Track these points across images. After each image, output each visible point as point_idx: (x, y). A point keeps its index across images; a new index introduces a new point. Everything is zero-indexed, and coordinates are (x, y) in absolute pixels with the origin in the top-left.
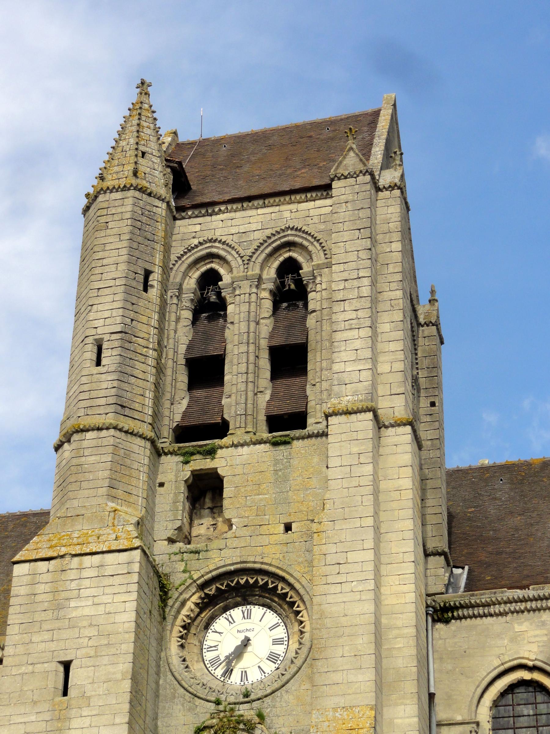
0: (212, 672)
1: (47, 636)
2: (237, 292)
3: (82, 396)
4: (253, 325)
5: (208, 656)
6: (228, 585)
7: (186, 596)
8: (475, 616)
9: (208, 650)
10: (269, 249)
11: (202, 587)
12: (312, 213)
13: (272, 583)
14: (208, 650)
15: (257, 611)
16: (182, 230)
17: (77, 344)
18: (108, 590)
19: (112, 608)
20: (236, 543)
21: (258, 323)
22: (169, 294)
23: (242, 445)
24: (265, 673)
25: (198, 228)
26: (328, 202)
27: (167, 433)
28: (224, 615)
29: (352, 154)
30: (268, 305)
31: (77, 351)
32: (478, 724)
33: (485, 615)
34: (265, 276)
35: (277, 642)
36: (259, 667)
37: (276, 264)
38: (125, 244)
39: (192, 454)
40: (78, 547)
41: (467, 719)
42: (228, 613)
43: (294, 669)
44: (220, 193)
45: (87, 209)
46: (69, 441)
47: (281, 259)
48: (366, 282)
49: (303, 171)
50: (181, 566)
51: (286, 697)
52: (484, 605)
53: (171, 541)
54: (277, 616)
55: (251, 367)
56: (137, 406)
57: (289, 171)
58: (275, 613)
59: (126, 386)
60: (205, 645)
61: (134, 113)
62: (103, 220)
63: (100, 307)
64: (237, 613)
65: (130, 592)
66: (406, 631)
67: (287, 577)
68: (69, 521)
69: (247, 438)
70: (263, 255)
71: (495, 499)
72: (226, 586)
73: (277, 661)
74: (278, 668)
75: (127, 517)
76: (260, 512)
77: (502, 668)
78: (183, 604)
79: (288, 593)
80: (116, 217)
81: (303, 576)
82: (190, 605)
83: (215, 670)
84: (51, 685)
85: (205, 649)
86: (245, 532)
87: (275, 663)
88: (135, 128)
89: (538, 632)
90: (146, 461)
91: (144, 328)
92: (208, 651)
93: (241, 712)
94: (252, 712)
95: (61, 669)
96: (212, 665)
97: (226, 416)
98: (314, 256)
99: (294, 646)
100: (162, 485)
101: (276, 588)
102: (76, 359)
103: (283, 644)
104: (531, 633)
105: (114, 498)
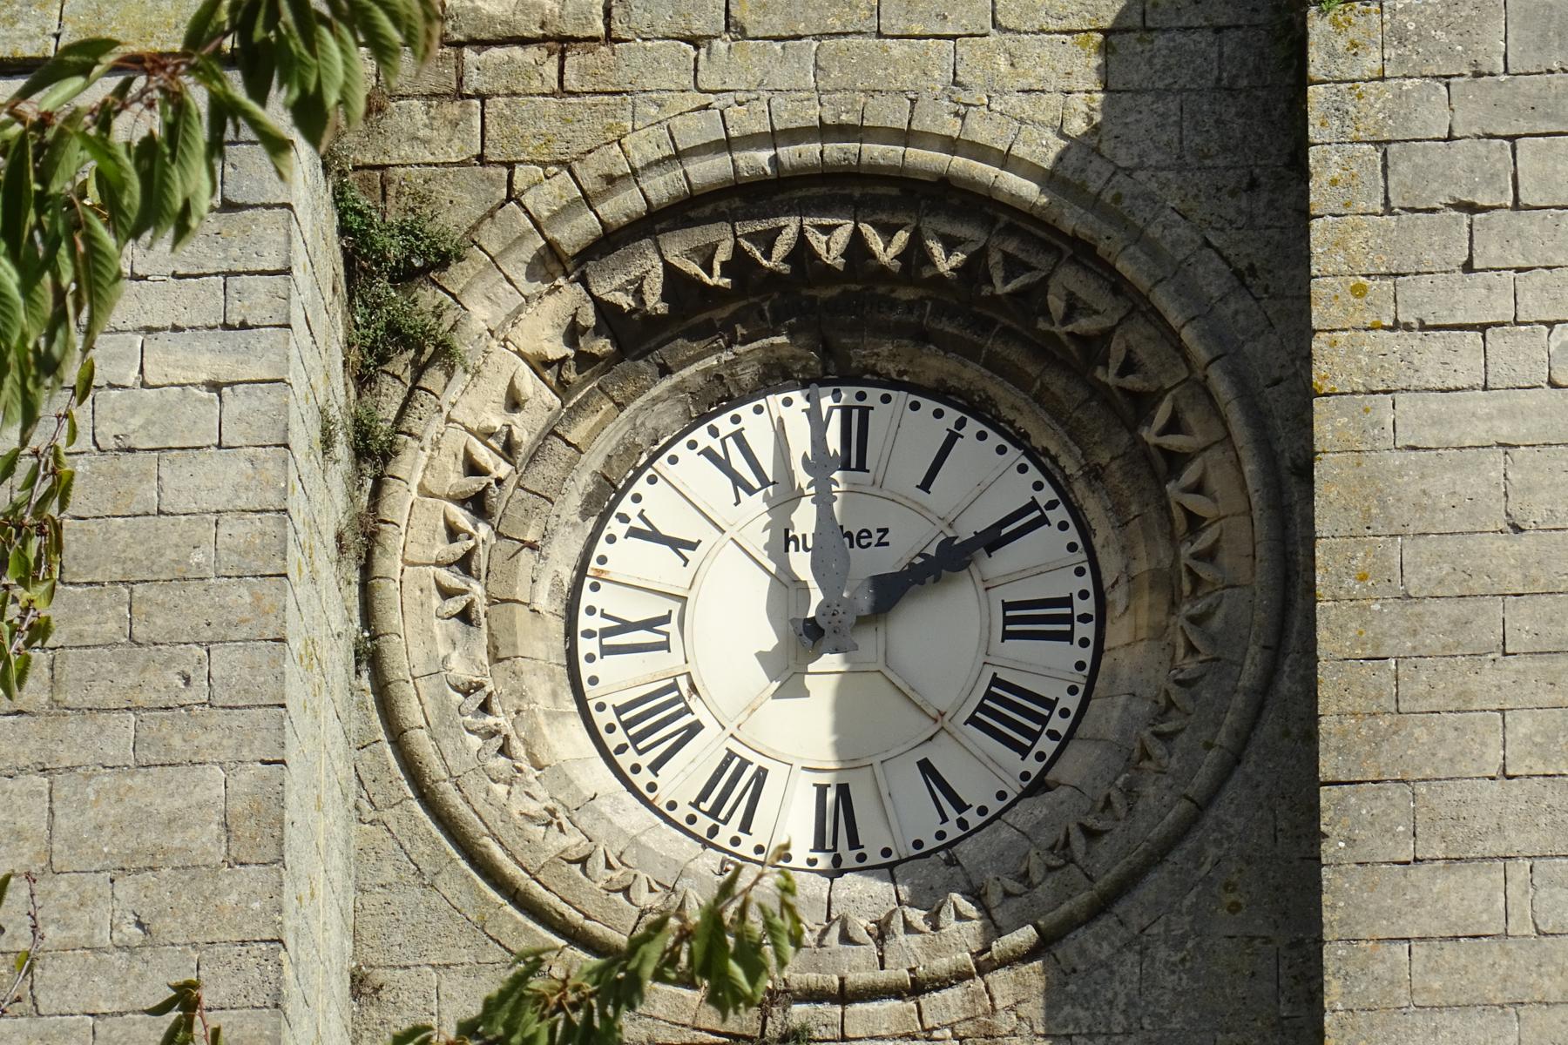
0: (641, 781)
6: (739, 265)
9: (607, 641)
14: (606, 641)
19: (135, 422)
24: (960, 806)
28: (701, 435)
36: (926, 767)
42: (723, 423)
54: (1025, 460)
58: (1017, 444)
60: (591, 611)
65: (244, 326)
67: (1109, 241)
72: (726, 269)
73: (1034, 736)
74: (1037, 786)
79: (1106, 335)
81: (1207, 244)
85: (589, 634)
87: (1024, 751)
92: (607, 651)
96: (635, 739)
101: (1031, 300)
103: (1068, 637)
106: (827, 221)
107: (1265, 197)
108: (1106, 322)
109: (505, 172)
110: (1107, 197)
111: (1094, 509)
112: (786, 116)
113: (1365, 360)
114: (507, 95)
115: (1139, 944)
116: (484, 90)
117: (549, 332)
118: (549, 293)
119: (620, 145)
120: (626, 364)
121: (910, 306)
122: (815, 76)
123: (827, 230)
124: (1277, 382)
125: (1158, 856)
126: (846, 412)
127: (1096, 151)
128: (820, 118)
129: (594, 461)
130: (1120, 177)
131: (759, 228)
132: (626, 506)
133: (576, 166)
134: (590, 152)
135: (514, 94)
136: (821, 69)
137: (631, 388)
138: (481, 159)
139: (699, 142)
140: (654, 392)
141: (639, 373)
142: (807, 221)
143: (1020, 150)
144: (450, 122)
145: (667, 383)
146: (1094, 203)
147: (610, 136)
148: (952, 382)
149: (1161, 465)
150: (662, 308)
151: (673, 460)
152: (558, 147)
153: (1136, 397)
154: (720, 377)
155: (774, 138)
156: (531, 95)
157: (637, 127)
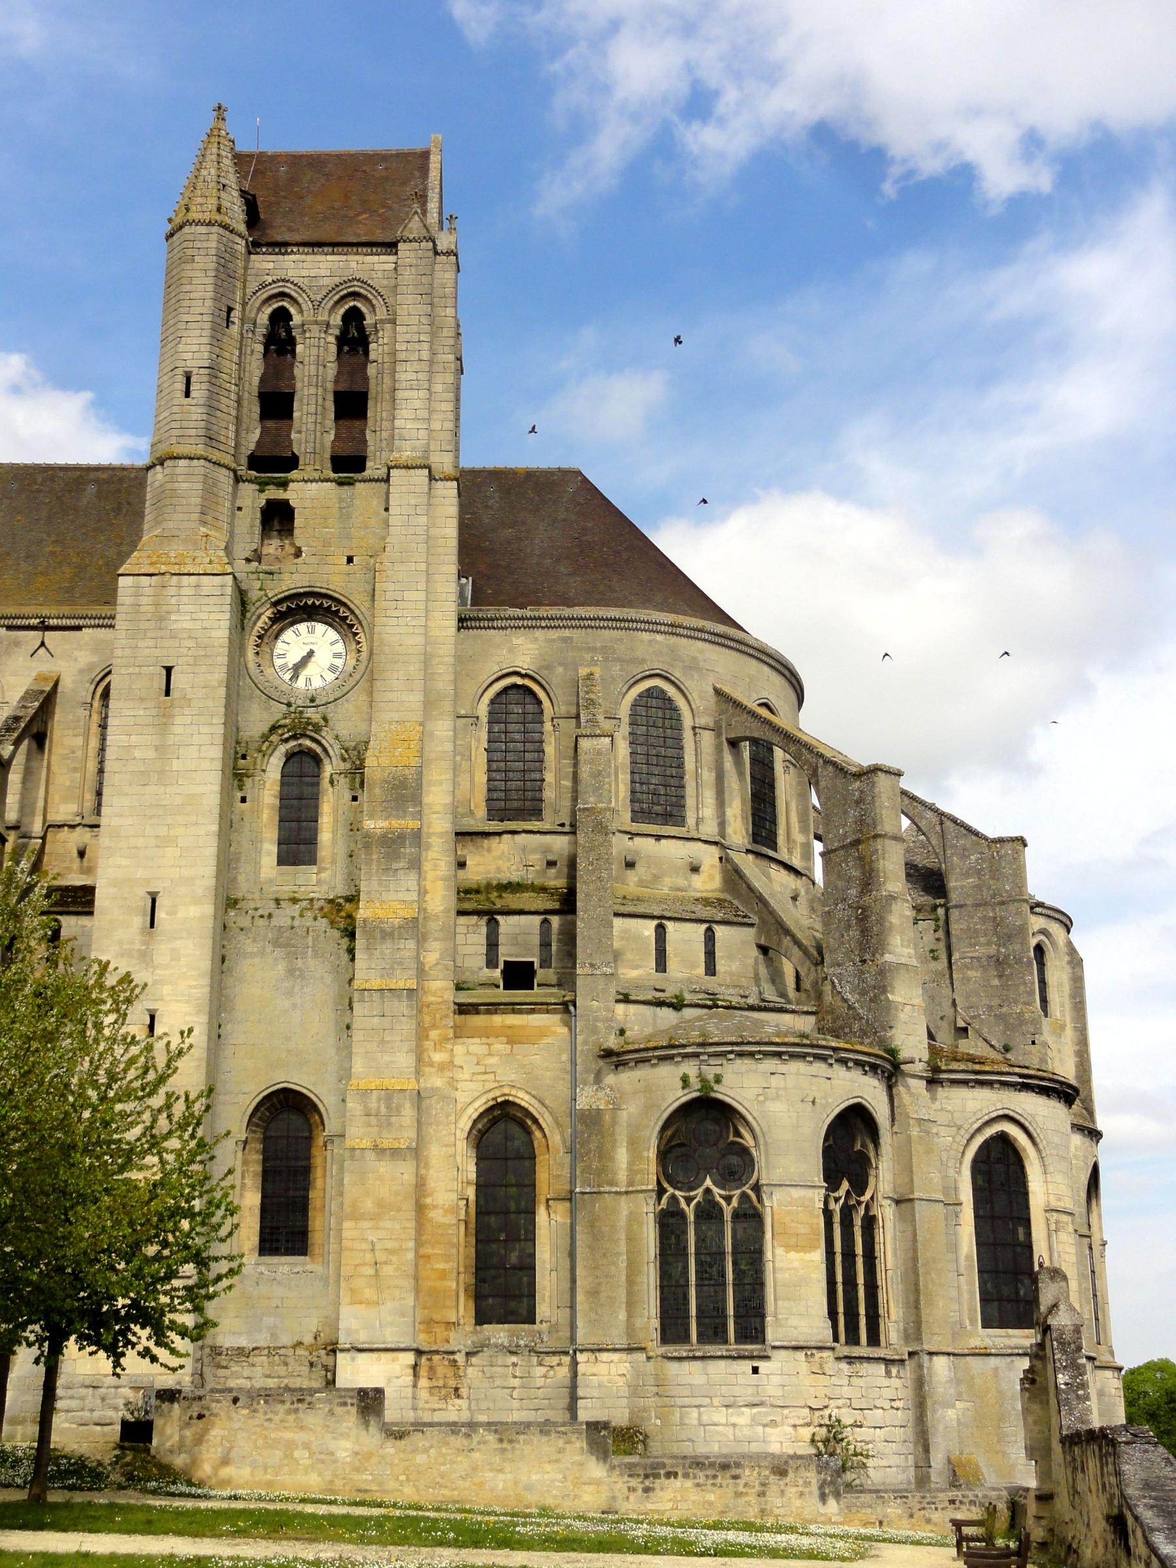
1: (151, 643)
2: (307, 335)
3: (174, 425)
4: (321, 368)
5: (278, 662)
7: (261, 611)
8: (480, 628)
10: (337, 297)
11: (275, 604)
12: (377, 267)
15: (320, 628)
16: (257, 265)
17: (165, 371)
18: (204, 608)
20: (304, 568)
21: (325, 367)
22: (245, 328)
23: (312, 481)
25: (271, 265)
26: (392, 258)
27: (244, 461)
29: (416, 217)
30: (333, 349)
31: (165, 378)
32: (477, 718)
33: (489, 628)
34: (332, 322)
35: (337, 655)
37: (342, 311)
38: (211, 280)
39: (267, 484)
40: (177, 567)
41: (469, 713)
43: (352, 682)
44: (290, 229)
45: (170, 236)
46: (162, 464)
47: (347, 307)
48: (426, 346)
49: (364, 216)
50: (257, 585)
51: (346, 705)
52: (489, 620)
53: (248, 560)
55: (319, 408)
56: (222, 439)
57: (351, 214)
59: (213, 420)
61: (213, 139)
62: (189, 252)
63: (189, 340)
64: (302, 627)
66: (446, 659)
67: (349, 603)
68: (165, 540)
69: (316, 475)
70: (332, 302)
71: (487, 507)
75: (218, 543)
76: (327, 543)
77: (500, 674)
78: (259, 617)
80: (202, 252)
82: (264, 618)
84: (156, 685)
86: (313, 560)
88: (214, 157)
89: (531, 646)
90: (230, 490)
91: (227, 363)
93: (309, 715)
94: (318, 716)
95: (164, 672)
97: (295, 451)
98: (377, 310)
99: (353, 662)
100: (240, 509)
101: (338, 611)
102: (165, 385)
104: (526, 647)
105: (204, 523)
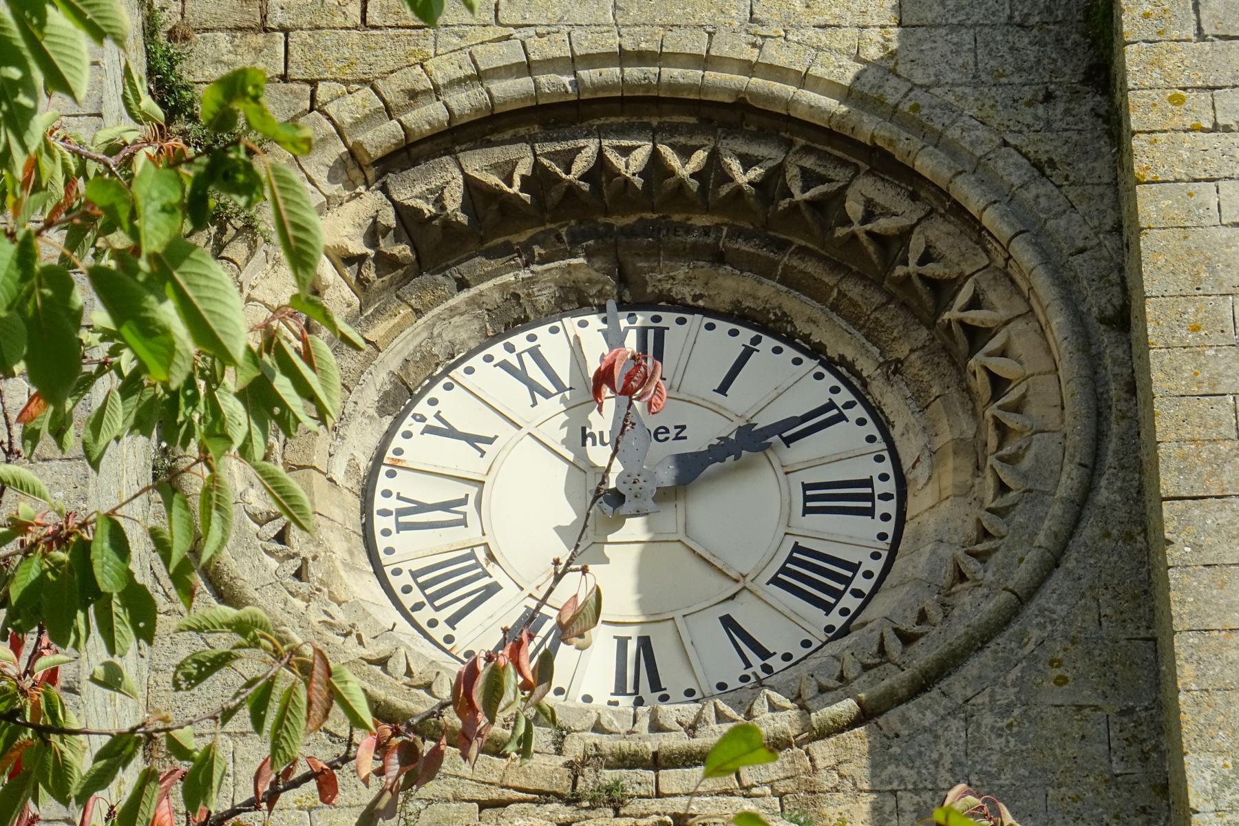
6: (539, 180)
9: (402, 519)
13: (809, 178)
14: (402, 519)
28: (498, 351)
36: (728, 622)
42: (520, 341)
54: (821, 369)
60: (386, 494)
67: (904, 145)
73: (838, 595)
79: (905, 235)
81: (1005, 144)
83: (452, 622)
85: (385, 513)
87: (828, 608)
92: (401, 527)
96: (432, 598)
103: (870, 512)
106: (625, 143)
107: (1061, 107)
108: (905, 222)
109: (308, 88)
110: (905, 107)
111: (892, 400)
112: (586, 44)
113: (1186, 155)
114: (310, 29)
115: (965, 712)
116: (288, 24)
117: (350, 230)
118: (352, 198)
119: (422, 66)
120: (426, 277)
121: (706, 231)
122: (614, 16)
123: (625, 151)
124: (1081, 251)
125: (979, 641)
126: (643, 333)
127: (893, 72)
128: (620, 46)
129: (390, 361)
130: (917, 91)
131: (558, 148)
132: (422, 407)
133: (380, 84)
134: (392, 72)
135: (318, 28)
136: (621, 9)
137: (428, 297)
138: (284, 78)
139: (501, 64)
140: (452, 302)
141: (437, 285)
142: (605, 142)
143: (817, 71)
144: (254, 49)
145: (465, 295)
146: (893, 114)
147: (413, 60)
148: (748, 303)
149: (963, 344)
150: (462, 218)
151: (469, 371)
152: (360, 70)
153: (935, 285)
154: (516, 296)
155: (573, 63)
156: (334, 28)
157: (439, 52)
